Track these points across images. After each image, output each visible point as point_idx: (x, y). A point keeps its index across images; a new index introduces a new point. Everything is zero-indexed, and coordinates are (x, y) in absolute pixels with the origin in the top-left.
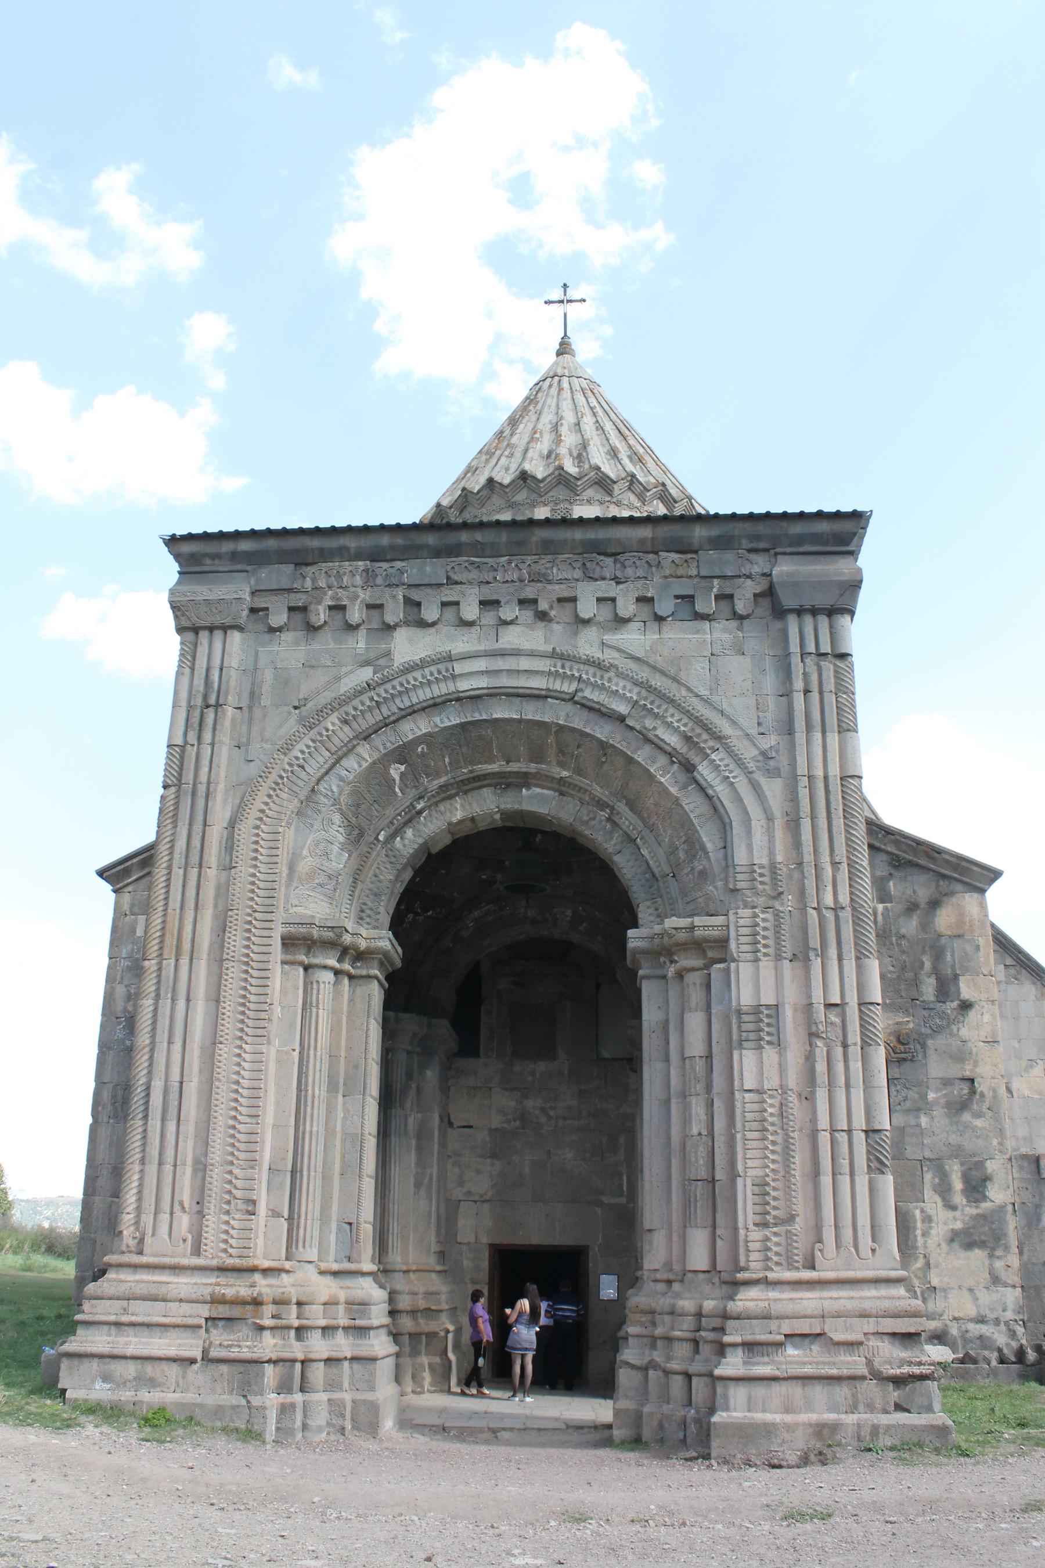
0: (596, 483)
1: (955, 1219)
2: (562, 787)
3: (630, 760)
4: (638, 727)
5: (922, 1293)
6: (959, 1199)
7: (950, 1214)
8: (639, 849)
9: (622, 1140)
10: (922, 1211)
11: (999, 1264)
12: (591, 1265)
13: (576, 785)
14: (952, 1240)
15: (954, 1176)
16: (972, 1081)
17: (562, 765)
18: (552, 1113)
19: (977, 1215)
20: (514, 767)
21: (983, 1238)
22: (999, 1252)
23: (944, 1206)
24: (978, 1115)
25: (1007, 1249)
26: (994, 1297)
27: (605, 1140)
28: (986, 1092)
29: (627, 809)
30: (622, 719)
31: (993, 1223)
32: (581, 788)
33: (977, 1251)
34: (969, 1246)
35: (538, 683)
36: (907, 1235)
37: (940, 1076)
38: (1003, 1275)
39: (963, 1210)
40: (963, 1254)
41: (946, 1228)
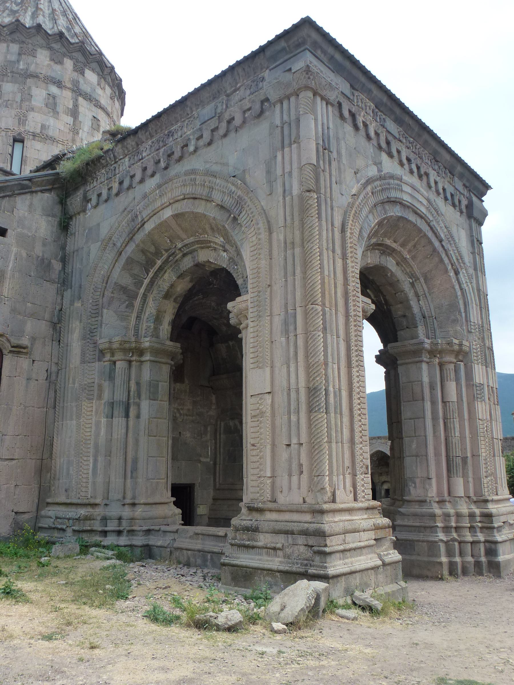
0: (97, 62)
2: (401, 262)
3: (441, 260)
4: (446, 248)
8: (419, 301)
9: (209, 429)
12: (196, 494)
13: (408, 263)
17: (409, 252)
18: (182, 412)
20: (394, 245)
27: (202, 429)
29: (423, 281)
30: (441, 241)
32: (410, 265)
35: (423, 210)
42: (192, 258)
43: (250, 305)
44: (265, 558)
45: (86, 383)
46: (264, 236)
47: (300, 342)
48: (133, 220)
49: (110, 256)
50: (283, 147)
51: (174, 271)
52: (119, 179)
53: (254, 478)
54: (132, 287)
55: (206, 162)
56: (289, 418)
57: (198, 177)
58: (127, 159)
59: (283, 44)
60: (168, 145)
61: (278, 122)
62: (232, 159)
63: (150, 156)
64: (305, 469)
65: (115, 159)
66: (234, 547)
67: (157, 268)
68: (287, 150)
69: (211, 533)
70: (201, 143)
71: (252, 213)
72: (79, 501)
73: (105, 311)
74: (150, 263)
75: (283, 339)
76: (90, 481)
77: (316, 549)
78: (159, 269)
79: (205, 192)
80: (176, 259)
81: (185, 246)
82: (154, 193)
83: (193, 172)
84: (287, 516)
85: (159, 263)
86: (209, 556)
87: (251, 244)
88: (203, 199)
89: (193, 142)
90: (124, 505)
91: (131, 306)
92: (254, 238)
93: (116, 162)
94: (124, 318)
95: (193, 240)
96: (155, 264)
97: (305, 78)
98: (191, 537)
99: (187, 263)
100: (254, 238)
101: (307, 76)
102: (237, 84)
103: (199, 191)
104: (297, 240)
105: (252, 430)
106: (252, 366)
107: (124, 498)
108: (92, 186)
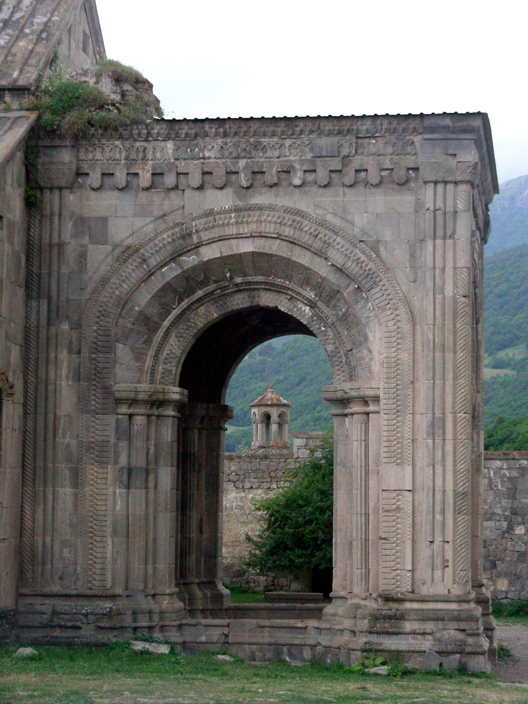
42: (249, 297)
43: (382, 397)
44: (411, 641)
45: (93, 440)
46: (406, 327)
47: (449, 447)
48: (183, 237)
49: (132, 272)
50: (435, 238)
51: (217, 307)
52: (154, 168)
53: (388, 570)
54: (155, 319)
55: (317, 206)
56: (434, 517)
57: (306, 222)
58: (170, 145)
59: (448, 121)
60: (253, 160)
61: (430, 204)
62: (361, 221)
63: (219, 161)
64: (450, 564)
65: (148, 136)
66: (373, 635)
67: (195, 299)
68: (439, 242)
69: (284, 625)
70: (310, 177)
71: (389, 295)
72: (89, 592)
73: (120, 346)
74: (189, 291)
75: (430, 441)
76: (109, 567)
77: (469, 632)
78: (197, 300)
79: (317, 245)
80: (224, 292)
81: (246, 283)
82: (228, 215)
83: (299, 213)
84: (431, 606)
85: (200, 293)
86: (285, 649)
87: (385, 329)
88: (310, 250)
89: (299, 174)
90: (146, 596)
91: (148, 342)
92: (391, 324)
93: (146, 140)
94: (139, 356)
95: (263, 280)
96: (194, 293)
97: (470, 172)
98: (250, 630)
99: (239, 302)
100: (391, 324)
101: (473, 171)
102: (376, 133)
103: (306, 239)
104: (449, 342)
105: (384, 524)
106: (385, 460)
107: (146, 587)
108: (90, 156)
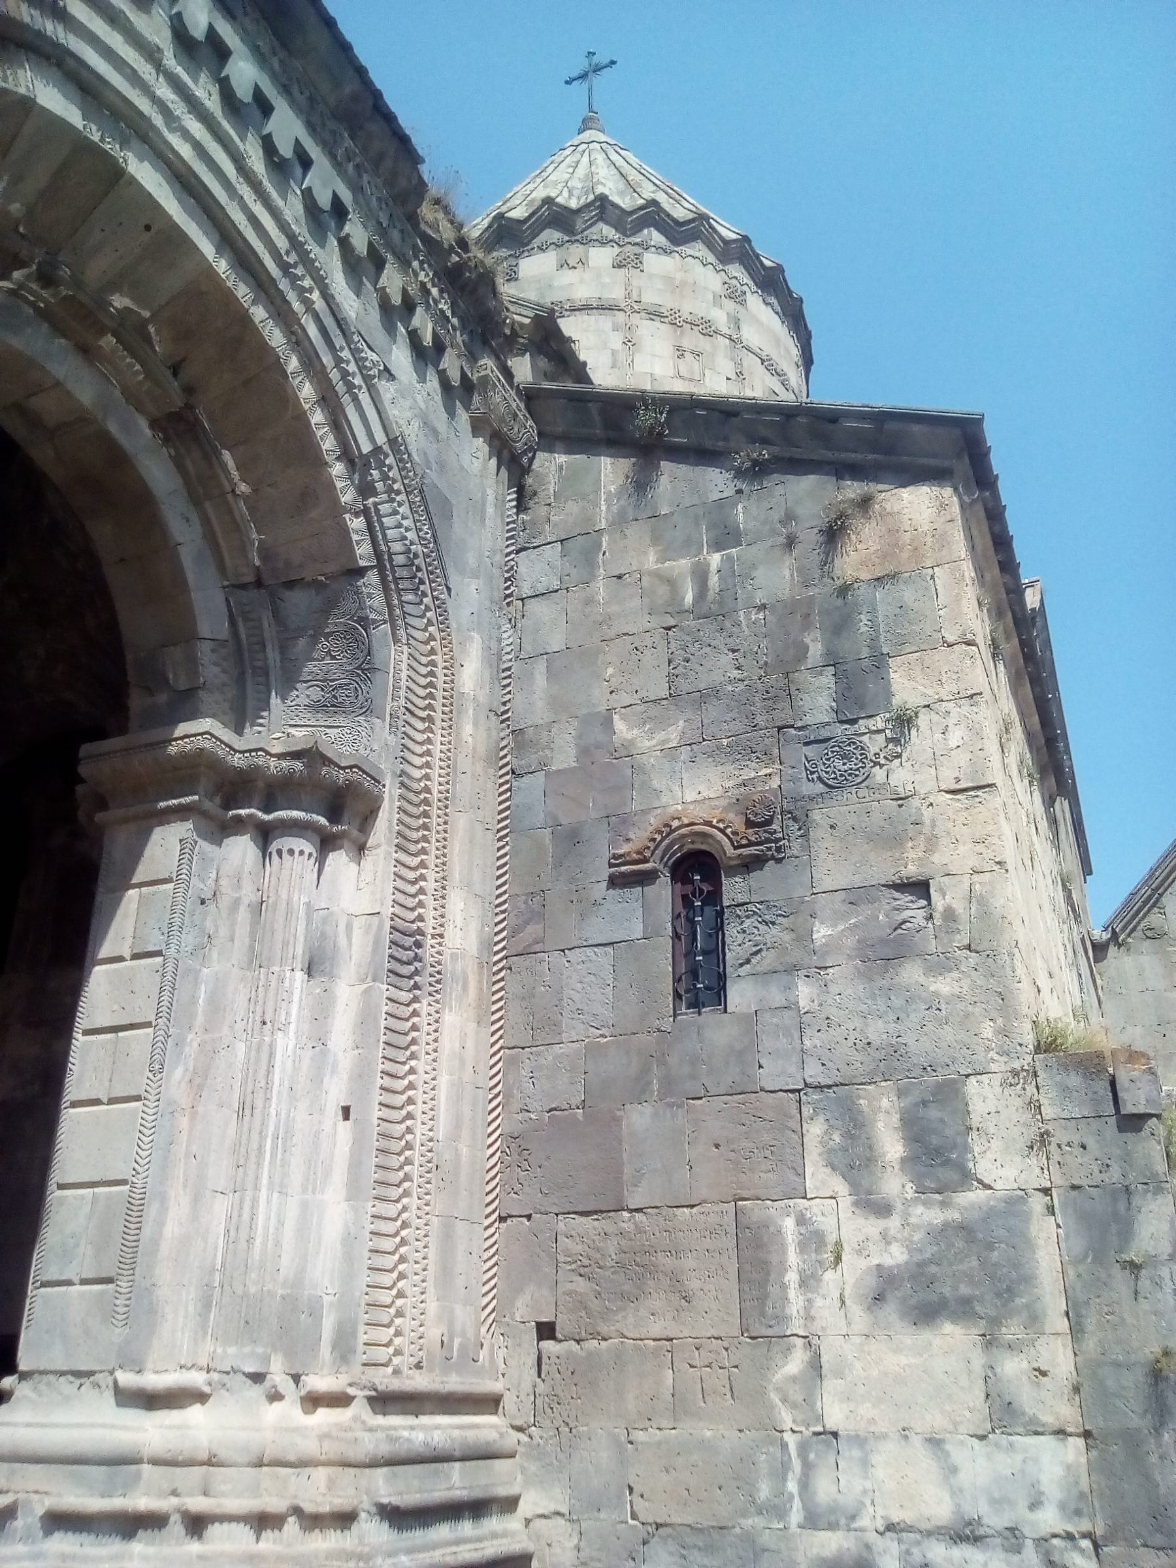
1: (886, 1239)
5: (803, 1449)
6: (895, 1184)
7: (872, 1227)
10: (801, 1221)
11: (1012, 1367)
14: (879, 1298)
15: (880, 1125)
16: (920, 888)
19: (946, 1226)
21: (965, 1290)
22: (1011, 1331)
23: (856, 1204)
24: (941, 965)
25: (1034, 1320)
26: (1005, 1464)
28: (959, 907)
31: (990, 1247)
33: (948, 1327)
34: (927, 1313)
36: (763, 1284)
37: (843, 883)
38: (1027, 1398)
39: (906, 1215)
40: (908, 1336)
41: (863, 1264)
